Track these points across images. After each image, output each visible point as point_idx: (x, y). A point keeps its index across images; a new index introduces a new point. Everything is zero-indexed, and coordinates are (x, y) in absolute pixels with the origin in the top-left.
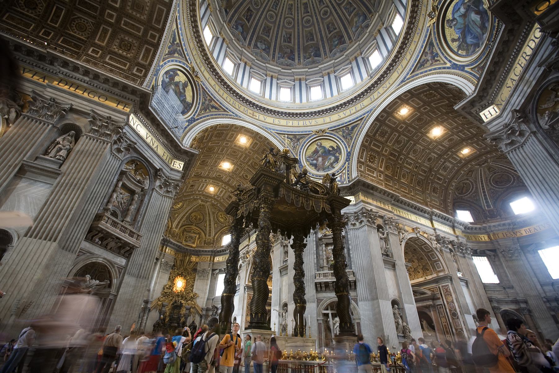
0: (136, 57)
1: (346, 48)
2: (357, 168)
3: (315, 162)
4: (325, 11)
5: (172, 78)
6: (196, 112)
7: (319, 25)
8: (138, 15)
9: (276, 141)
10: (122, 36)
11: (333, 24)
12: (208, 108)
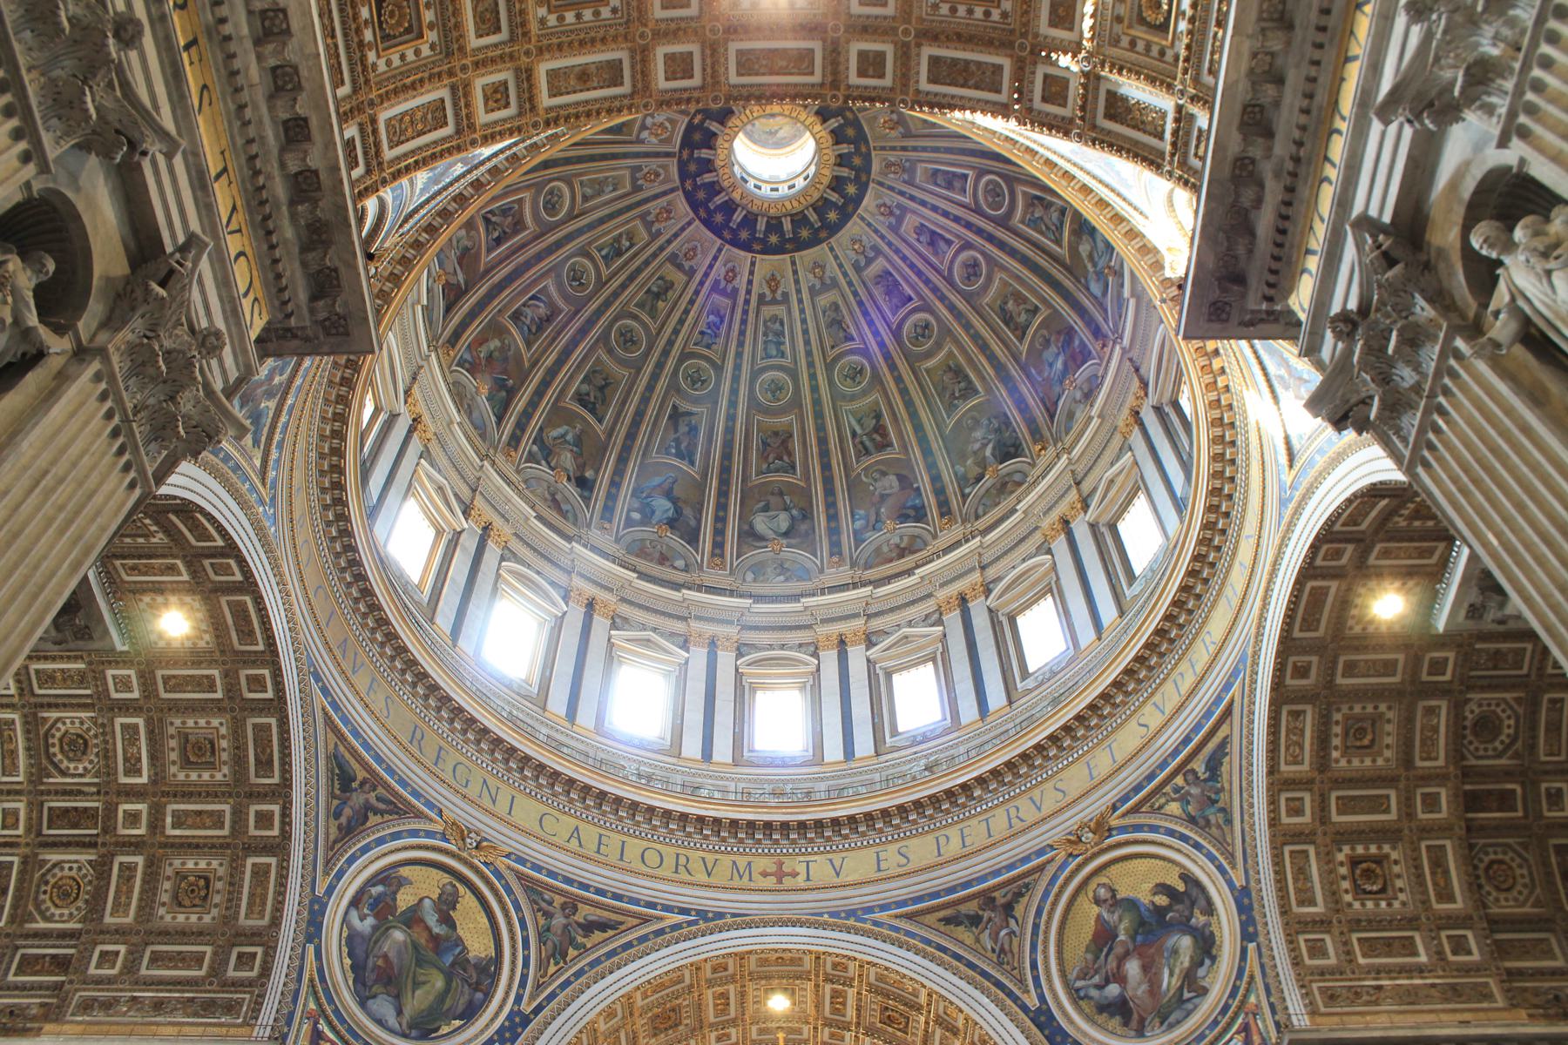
0: (229, 918)
1: (1096, 376)
2: (1296, 962)
3: (1113, 990)
4: (966, 265)
5: (383, 909)
6: (523, 984)
7: (967, 326)
8: (206, 776)
9: (910, 955)
10: (177, 863)
11: (1019, 299)
12: (572, 942)
